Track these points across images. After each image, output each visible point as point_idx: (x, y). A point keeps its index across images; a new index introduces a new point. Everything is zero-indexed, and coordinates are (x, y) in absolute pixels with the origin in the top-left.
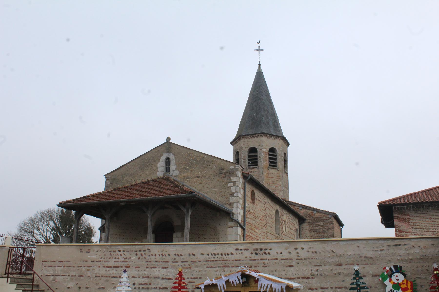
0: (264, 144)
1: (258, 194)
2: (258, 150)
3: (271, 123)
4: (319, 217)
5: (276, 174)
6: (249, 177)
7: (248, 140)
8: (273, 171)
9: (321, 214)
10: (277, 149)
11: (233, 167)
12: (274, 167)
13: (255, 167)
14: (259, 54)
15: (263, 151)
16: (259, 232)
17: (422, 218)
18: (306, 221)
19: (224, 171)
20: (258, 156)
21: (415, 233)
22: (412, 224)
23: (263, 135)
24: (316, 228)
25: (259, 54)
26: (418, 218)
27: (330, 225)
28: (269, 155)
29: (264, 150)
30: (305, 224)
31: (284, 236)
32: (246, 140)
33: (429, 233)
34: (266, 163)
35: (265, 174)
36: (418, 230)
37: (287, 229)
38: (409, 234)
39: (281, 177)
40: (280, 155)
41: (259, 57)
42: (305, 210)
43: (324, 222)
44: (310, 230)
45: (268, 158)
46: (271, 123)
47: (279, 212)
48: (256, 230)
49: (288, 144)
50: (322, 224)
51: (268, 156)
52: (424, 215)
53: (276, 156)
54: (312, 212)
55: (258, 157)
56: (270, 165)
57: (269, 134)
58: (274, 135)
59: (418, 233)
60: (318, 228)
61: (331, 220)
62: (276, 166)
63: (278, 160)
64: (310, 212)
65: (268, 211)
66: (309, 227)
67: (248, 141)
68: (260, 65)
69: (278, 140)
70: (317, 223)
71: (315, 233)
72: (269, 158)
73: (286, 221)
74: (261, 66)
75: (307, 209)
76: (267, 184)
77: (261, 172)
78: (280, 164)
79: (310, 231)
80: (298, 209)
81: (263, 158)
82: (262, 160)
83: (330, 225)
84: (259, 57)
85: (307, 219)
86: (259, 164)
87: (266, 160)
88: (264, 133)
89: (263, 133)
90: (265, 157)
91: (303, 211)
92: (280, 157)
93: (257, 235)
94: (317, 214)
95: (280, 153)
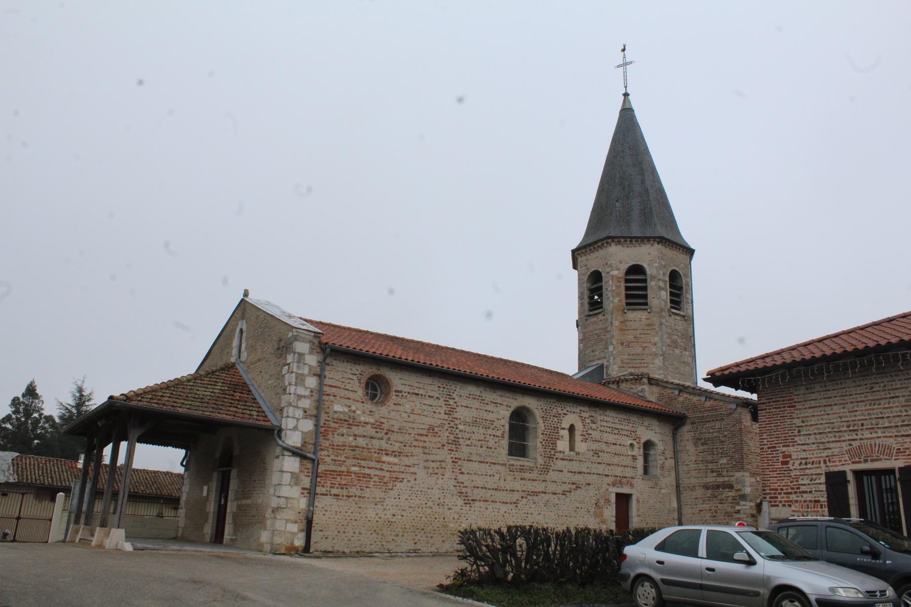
0: (617, 259)
1: (397, 380)
2: (603, 275)
3: (636, 213)
4: (713, 409)
5: (644, 321)
6: (328, 350)
7: (589, 257)
8: (637, 316)
9: (716, 403)
10: (645, 265)
11: (290, 334)
12: (638, 307)
13: (597, 311)
14: (625, 72)
15: (613, 276)
16: (406, 461)
17: (824, 402)
18: (689, 421)
19: (282, 344)
20: (604, 288)
21: (805, 447)
22: (798, 422)
23: (609, 241)
24: (707, 436)
25: (625, 72)
26: (813, 403)
27: (734, 426)
28: (627, 281)
29: (615, 273)
30: (686, 428)
31: (560, 464)
32: (584, 258)
33: (838, 444)
34: (620, 301)
35: (616, 323)
36: (812, 437)
37: (581, 446)
38: (791, 449)
39: (656, 327)
40: (653, 278)
41: (625, 80)
42: (686, 395)
43: (722, 420)
44: (697, 441)
45: (623, 288)
46: (636, 213)
47: (538, 414)
48: (385, 458)
49: (690, 252)
50: (718, 425)
51: (623, 285)
52: (829, 394)
53: (645, 281)
54: (699, 398)
55: (604, 290)
56: (628, 304)
57: (623, 237)
58: (637, 238)
59: (814, 447)
60: (710, 436)
61: (736, 415)
62: (646, 304)
63: (649, 292)
64: (695, 399)
65: (462, 413)
66: (692, 434)
67: (587, 260)
68: (626, 95)
69: (648, 246)
70: (708, 425)
71: (705, 447)
72: (627, 288)
73: (579, 427)
74: (630, 97)
75: (690, 394)
76: (622, 344)
77: (609, 320)
78: (659, 295)
79: (695, 444)
80: (672, 395)
81: (613, 291)
82: (610, 294)
83: (734, 426)
84: (625, 80)
85: (689, 414)
86: (606, 304)
87: (618, 294)
88: (613, 238)
89: (608, 237)
90: (617, 287)
91: (681, 399)
92: (653, 283)
93: (396, 468)
94: (708, 404)
95: (655, 272)
